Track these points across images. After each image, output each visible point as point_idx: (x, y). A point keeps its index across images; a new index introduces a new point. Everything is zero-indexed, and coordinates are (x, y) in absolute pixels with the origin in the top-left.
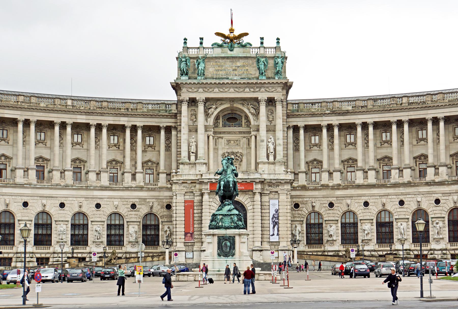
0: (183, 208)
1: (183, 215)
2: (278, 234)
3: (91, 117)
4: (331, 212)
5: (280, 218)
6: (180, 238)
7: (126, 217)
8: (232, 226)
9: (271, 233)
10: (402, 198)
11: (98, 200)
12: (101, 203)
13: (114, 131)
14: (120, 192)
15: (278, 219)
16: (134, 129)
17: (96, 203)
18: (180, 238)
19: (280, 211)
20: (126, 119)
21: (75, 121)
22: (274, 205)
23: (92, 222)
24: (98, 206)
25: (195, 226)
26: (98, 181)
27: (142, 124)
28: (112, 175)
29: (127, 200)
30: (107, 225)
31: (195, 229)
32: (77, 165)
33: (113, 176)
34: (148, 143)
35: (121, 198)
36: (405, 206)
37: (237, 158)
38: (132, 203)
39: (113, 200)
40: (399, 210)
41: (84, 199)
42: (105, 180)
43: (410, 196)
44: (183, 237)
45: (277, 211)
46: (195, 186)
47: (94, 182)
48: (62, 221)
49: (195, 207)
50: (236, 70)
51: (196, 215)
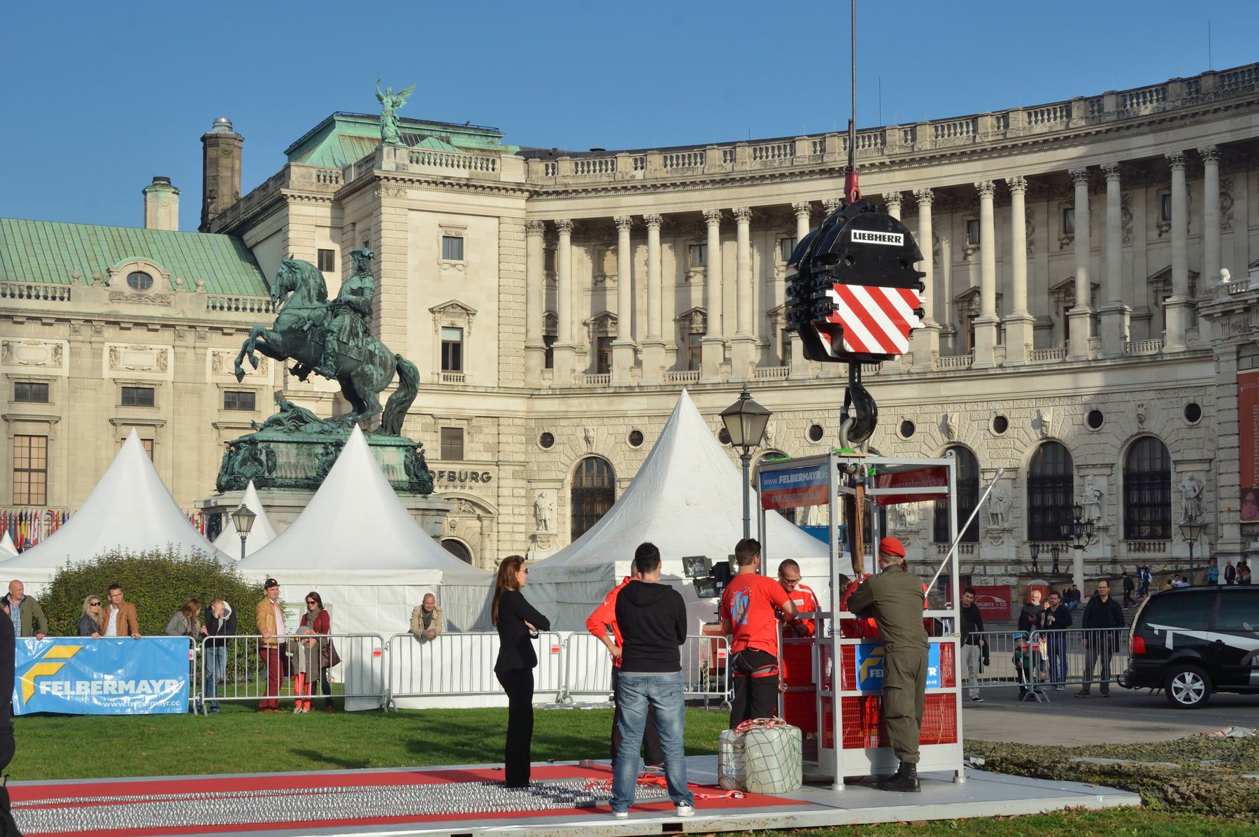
0: (1234, 402)
3: (1163, 136)
6: (1229, 510)
11: (1191, 393)
17: (1185, 402)
18: (1229, 510)
21: (1125, 157)
23: (1176, 462)
24: (1193, 412)
26: (1190, 335)
41: (1151, 395)
44: (1236, 504)
48: (1094, 466)
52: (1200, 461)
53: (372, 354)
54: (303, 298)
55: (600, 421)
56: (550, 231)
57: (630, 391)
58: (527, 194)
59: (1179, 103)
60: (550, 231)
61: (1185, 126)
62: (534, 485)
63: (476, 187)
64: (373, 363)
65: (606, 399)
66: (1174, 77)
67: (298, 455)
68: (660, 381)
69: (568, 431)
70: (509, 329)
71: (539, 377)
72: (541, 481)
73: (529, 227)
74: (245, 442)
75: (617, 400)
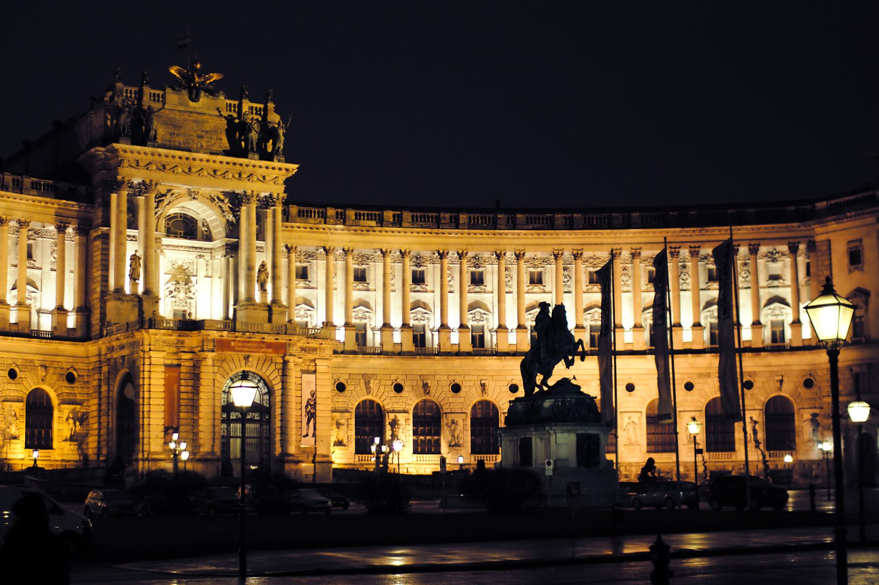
0: (162, 382)
1: (163, 395)
2: (314, 435)
4: (340, 399)
5: (318, 407)
9: (304, 433)
10: (458, 381)
15: (315, 408)
19: (318, 395)
22: (309, 383)
25: (182, 415)
31: (182, 422)
36: (461, 394)
37: (191, 295)
40: (451, 400)
43: (470, 378)
44: (162, 435)
45: (313, 394)
46: (183, 342)
49: (183, 382)
50: (202, 137)
51: (183, 396)
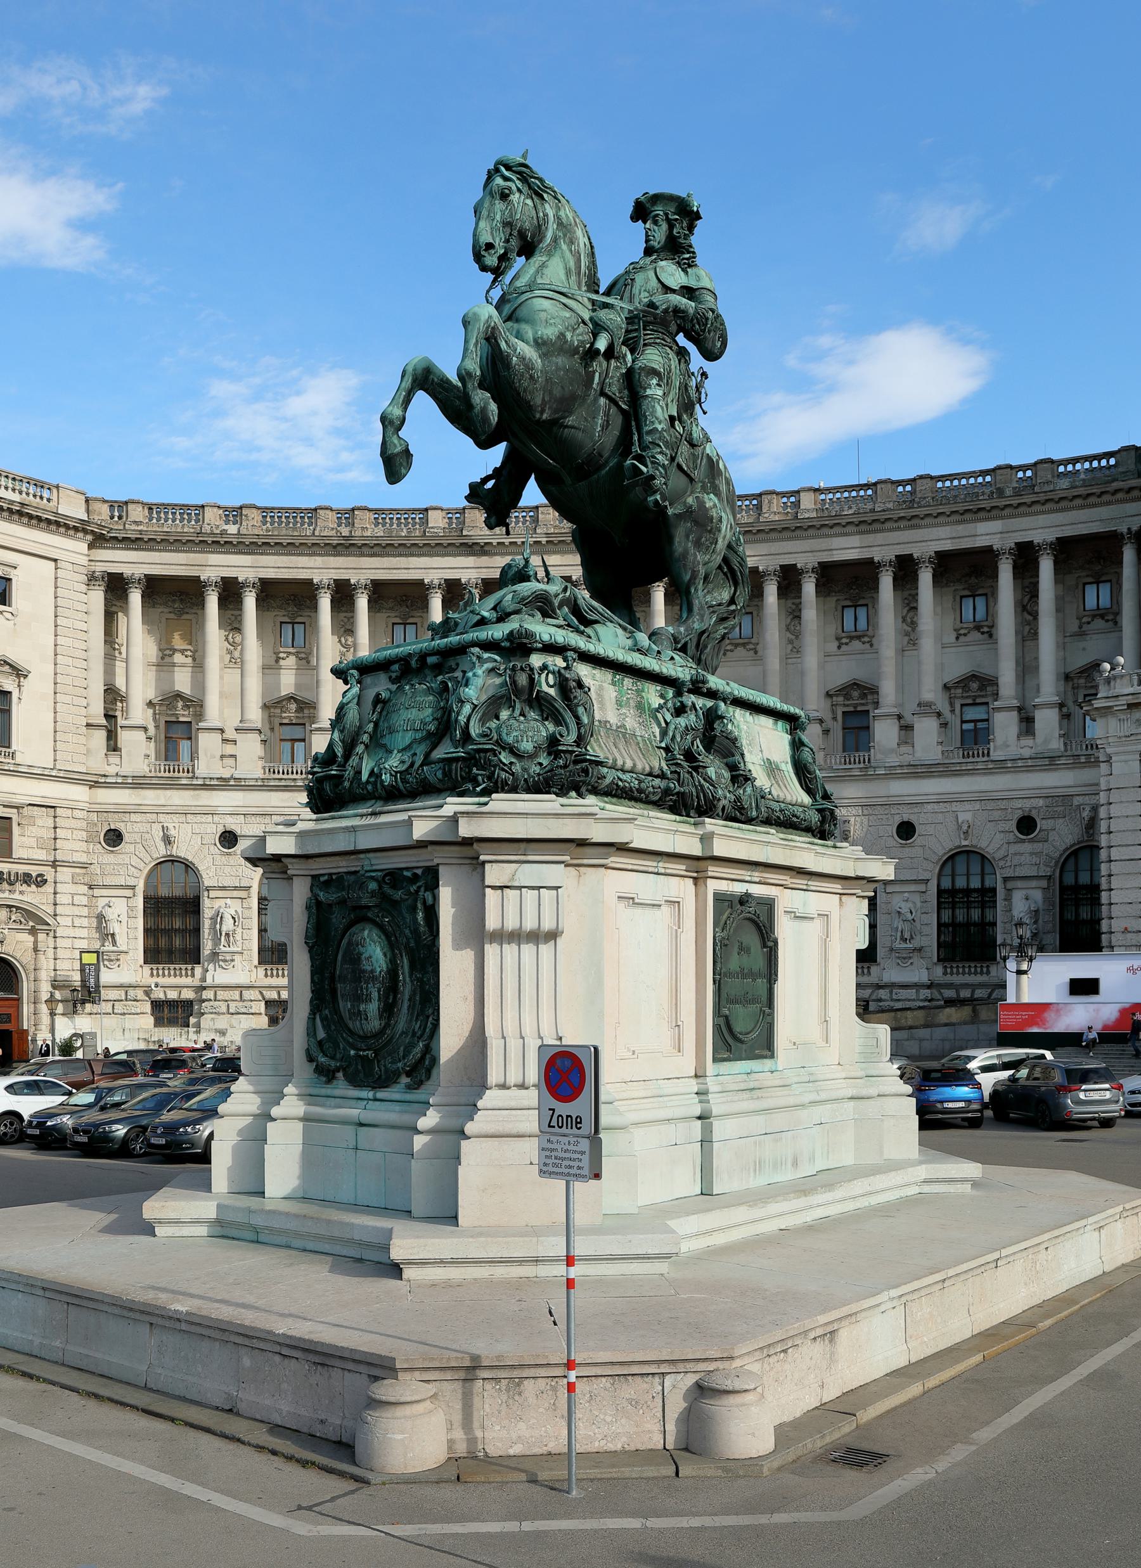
3: (870, 539)
7: (1001, 863)
8: (433, 774)
12: (914, 819)
13: (973, 580)
14: (978, 779)
16: (1025, 557)
17: (897, 820)
20: (995, 526)
26: (904, 749)
27: (1050, 536)
28: (971, 726)
29: (1002, 804)
30: (940, 892)
32: (855, 706)
33: (976, 729)
34: (1091, 602)
35: (983, 799)
38: (1018, 814)
39: (955, 807)
42: (928, 740)
47: (892, 751)
52: (915, 881)
53: (713, 467)
54: (568, 273)
55: (182, 818)
56: (116, 587)
57: (224, 784)
58: (90, 537)
59: (890, 506)
60: (116, 587)
61: (899, 529)
62: (97, 892)
63: (30, 517)
64: (718, 494)
65: (192, 793)
66: (883, 477)
67: (619, 704)
68: (259, 773)
69: (137, 827)
70: (68, 699)
71: (98, 762)
72: (105, 887)
73: (92, 578)
74: (489, 646)
75: (204, 794)
